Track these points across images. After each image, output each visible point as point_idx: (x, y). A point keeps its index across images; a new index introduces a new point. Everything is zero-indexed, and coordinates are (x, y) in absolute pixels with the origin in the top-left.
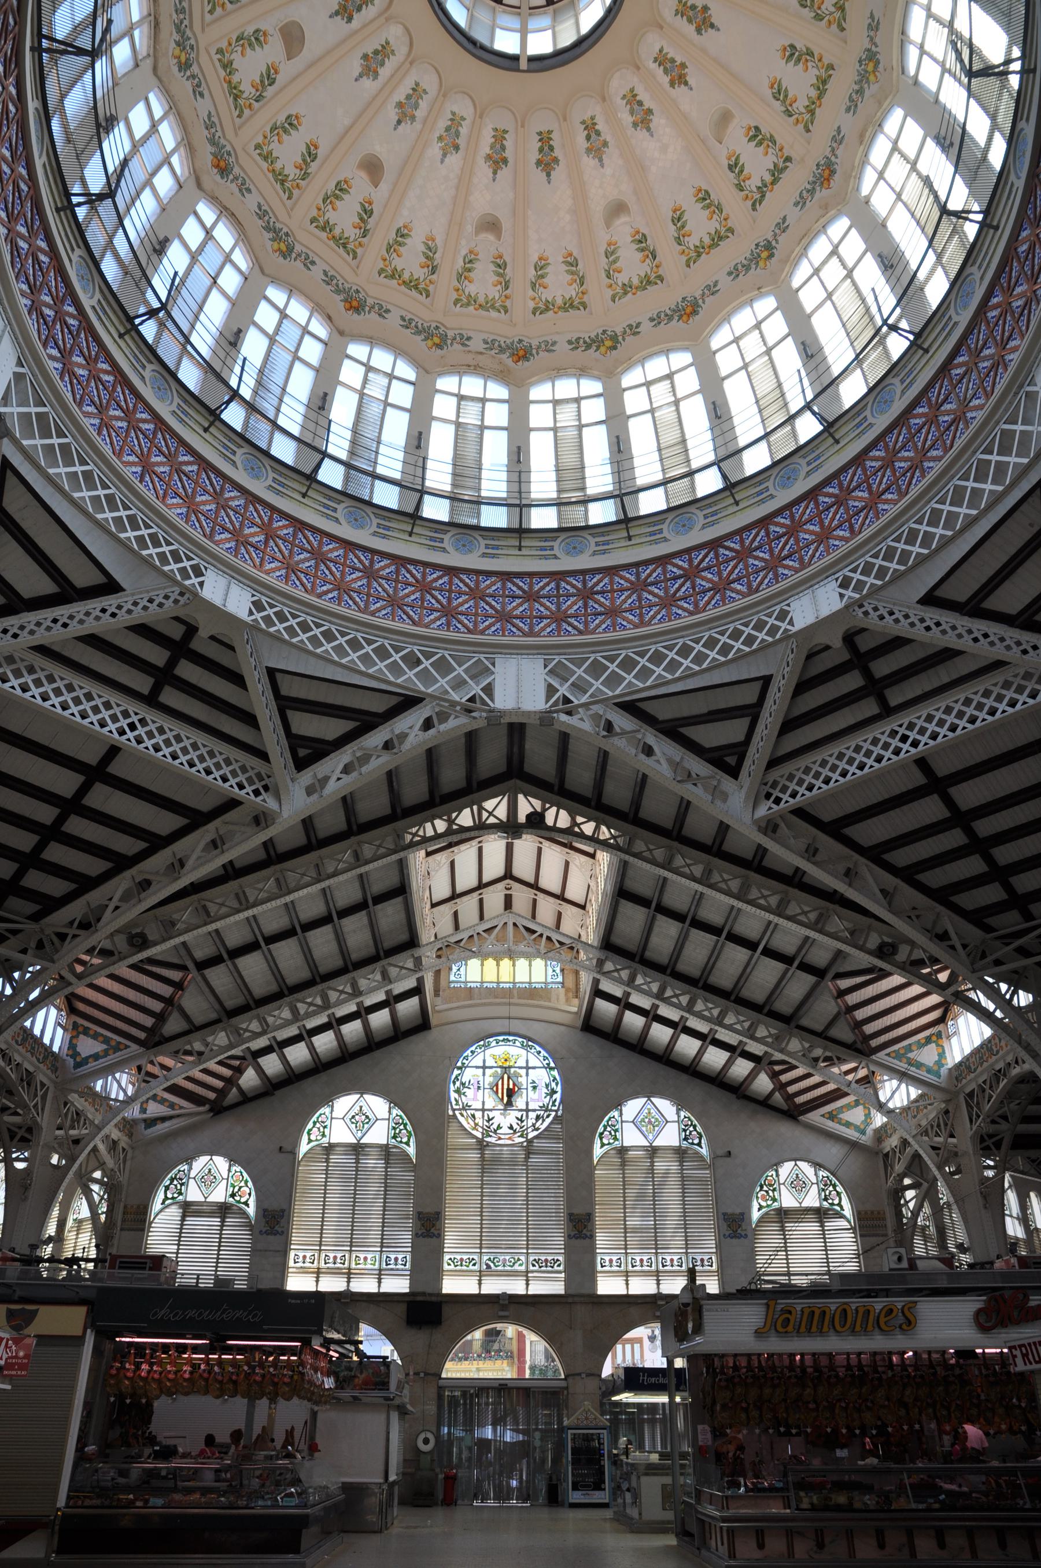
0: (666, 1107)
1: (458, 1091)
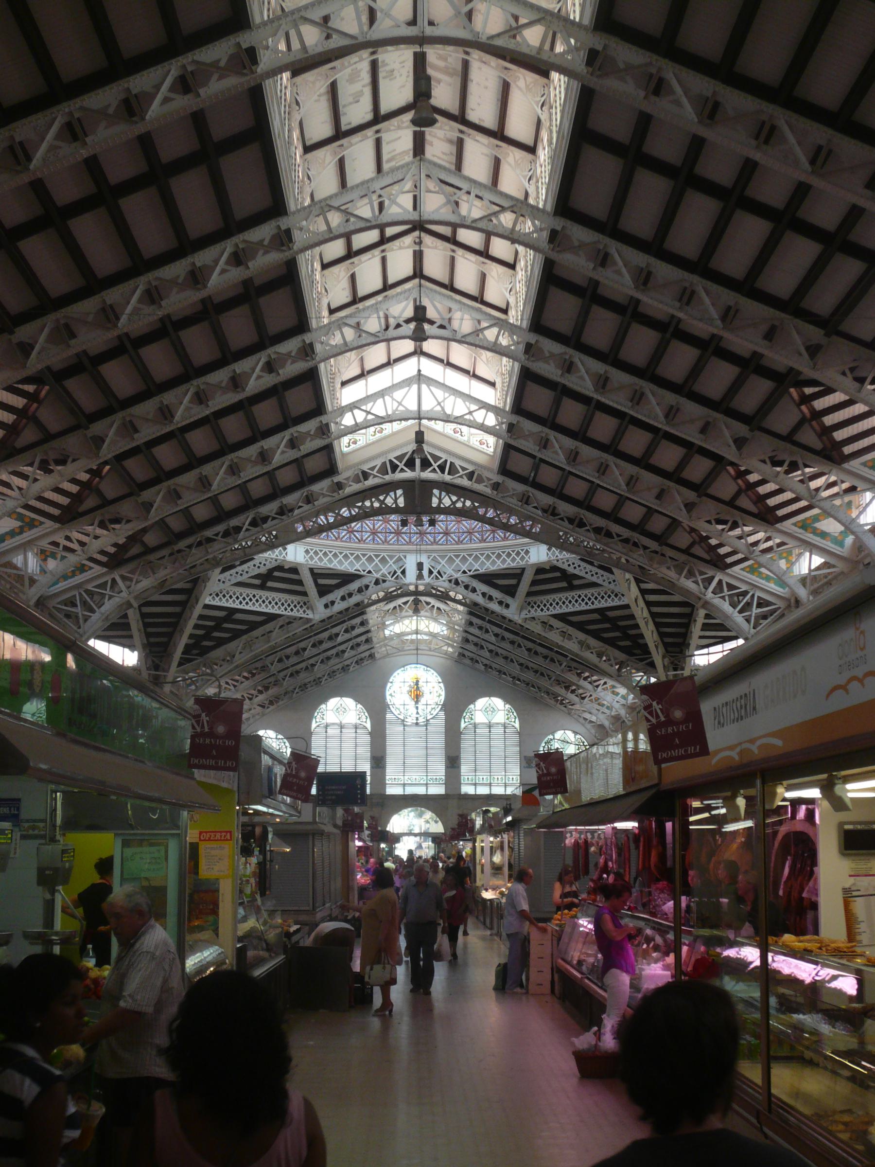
0: (498, 702)
1: (391, 695)
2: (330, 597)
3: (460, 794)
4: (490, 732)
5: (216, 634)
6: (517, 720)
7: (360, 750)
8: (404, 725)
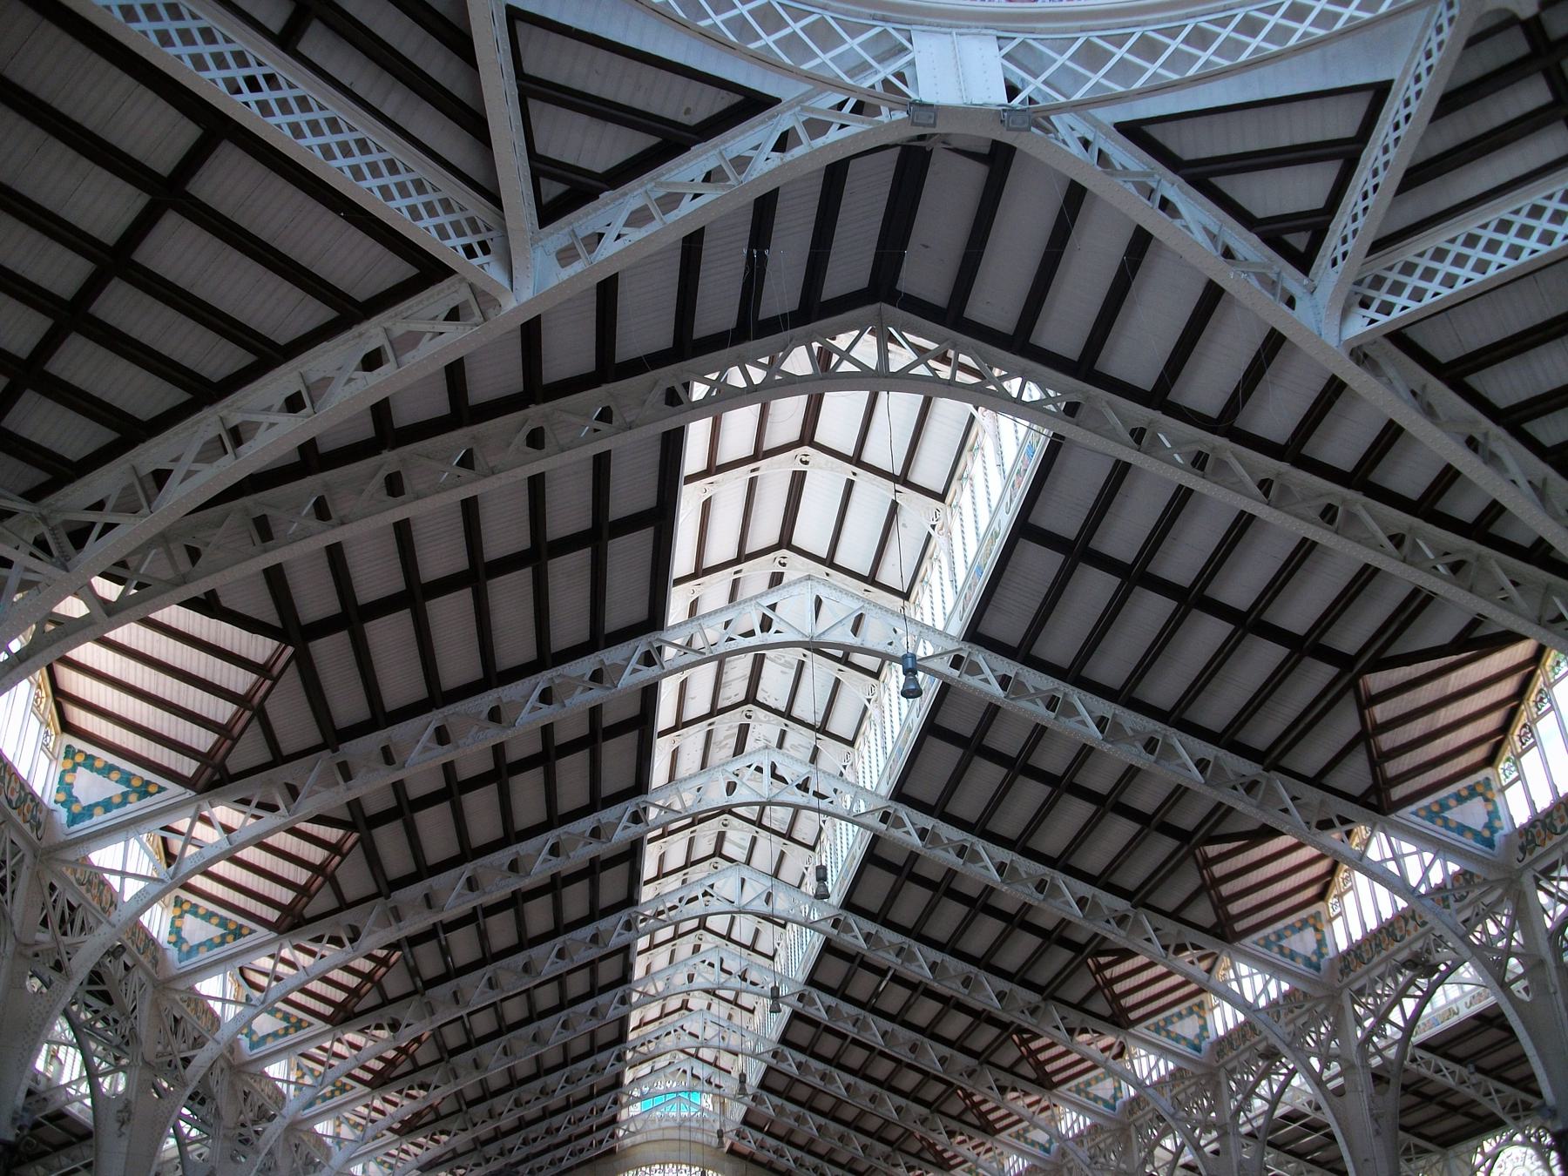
2: (585, 220)
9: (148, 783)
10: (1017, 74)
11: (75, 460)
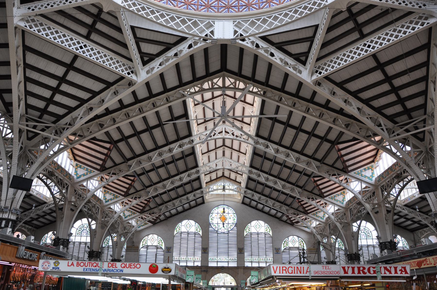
0: (262, 223)
3: (244, 267)
4: (258, 236)
5: (58, 98)
6: (271, 231)
7: (196, 245)
8: (218, 233)
9: (91, 170)
10: (237, 29)
11: (62, 115)
